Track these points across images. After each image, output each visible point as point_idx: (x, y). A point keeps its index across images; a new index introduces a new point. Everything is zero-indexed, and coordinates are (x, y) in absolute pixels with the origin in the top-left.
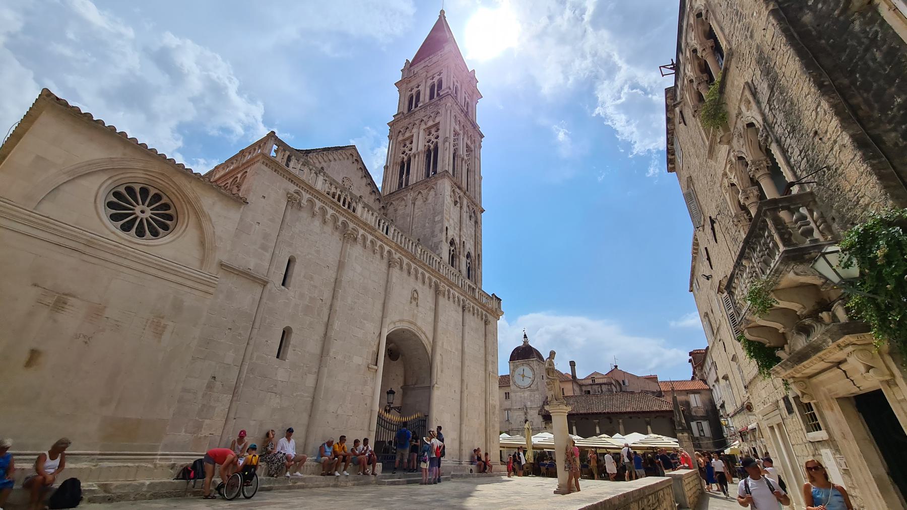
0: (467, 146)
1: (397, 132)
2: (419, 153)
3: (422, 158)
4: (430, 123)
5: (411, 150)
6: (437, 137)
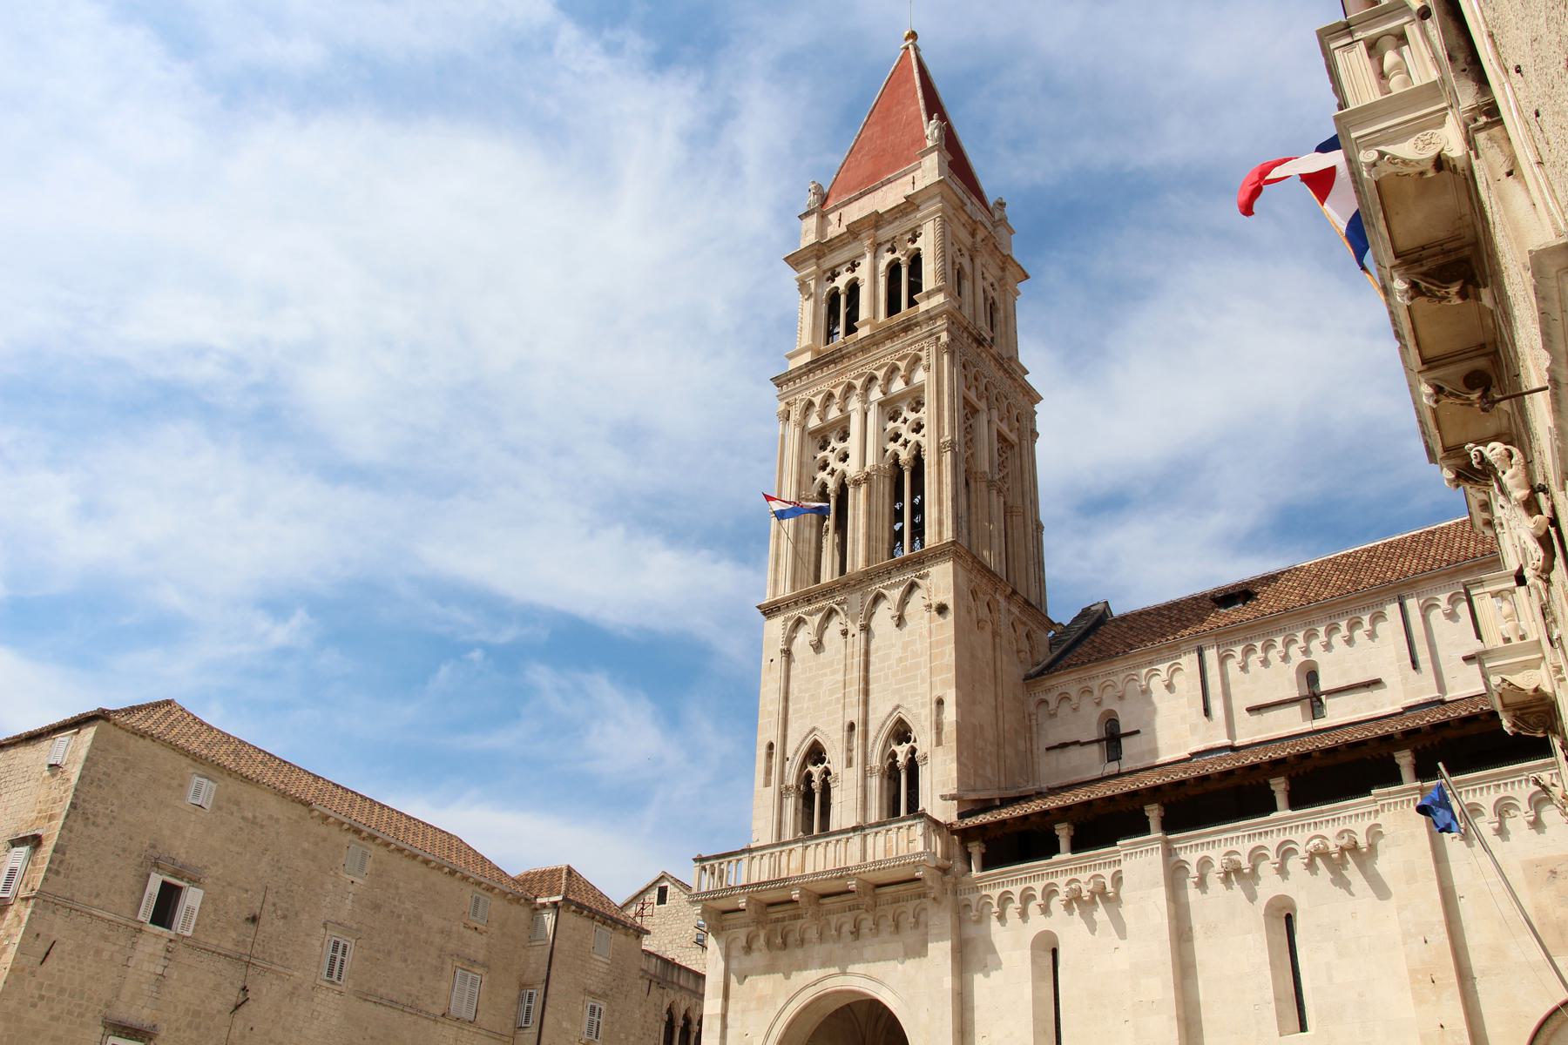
0: (1002, 438)
1: (799, 406)
2: (868, 477)
3: (884, 488)
4: (898, 386)
5: (845, 457)
6: (918, 428)
